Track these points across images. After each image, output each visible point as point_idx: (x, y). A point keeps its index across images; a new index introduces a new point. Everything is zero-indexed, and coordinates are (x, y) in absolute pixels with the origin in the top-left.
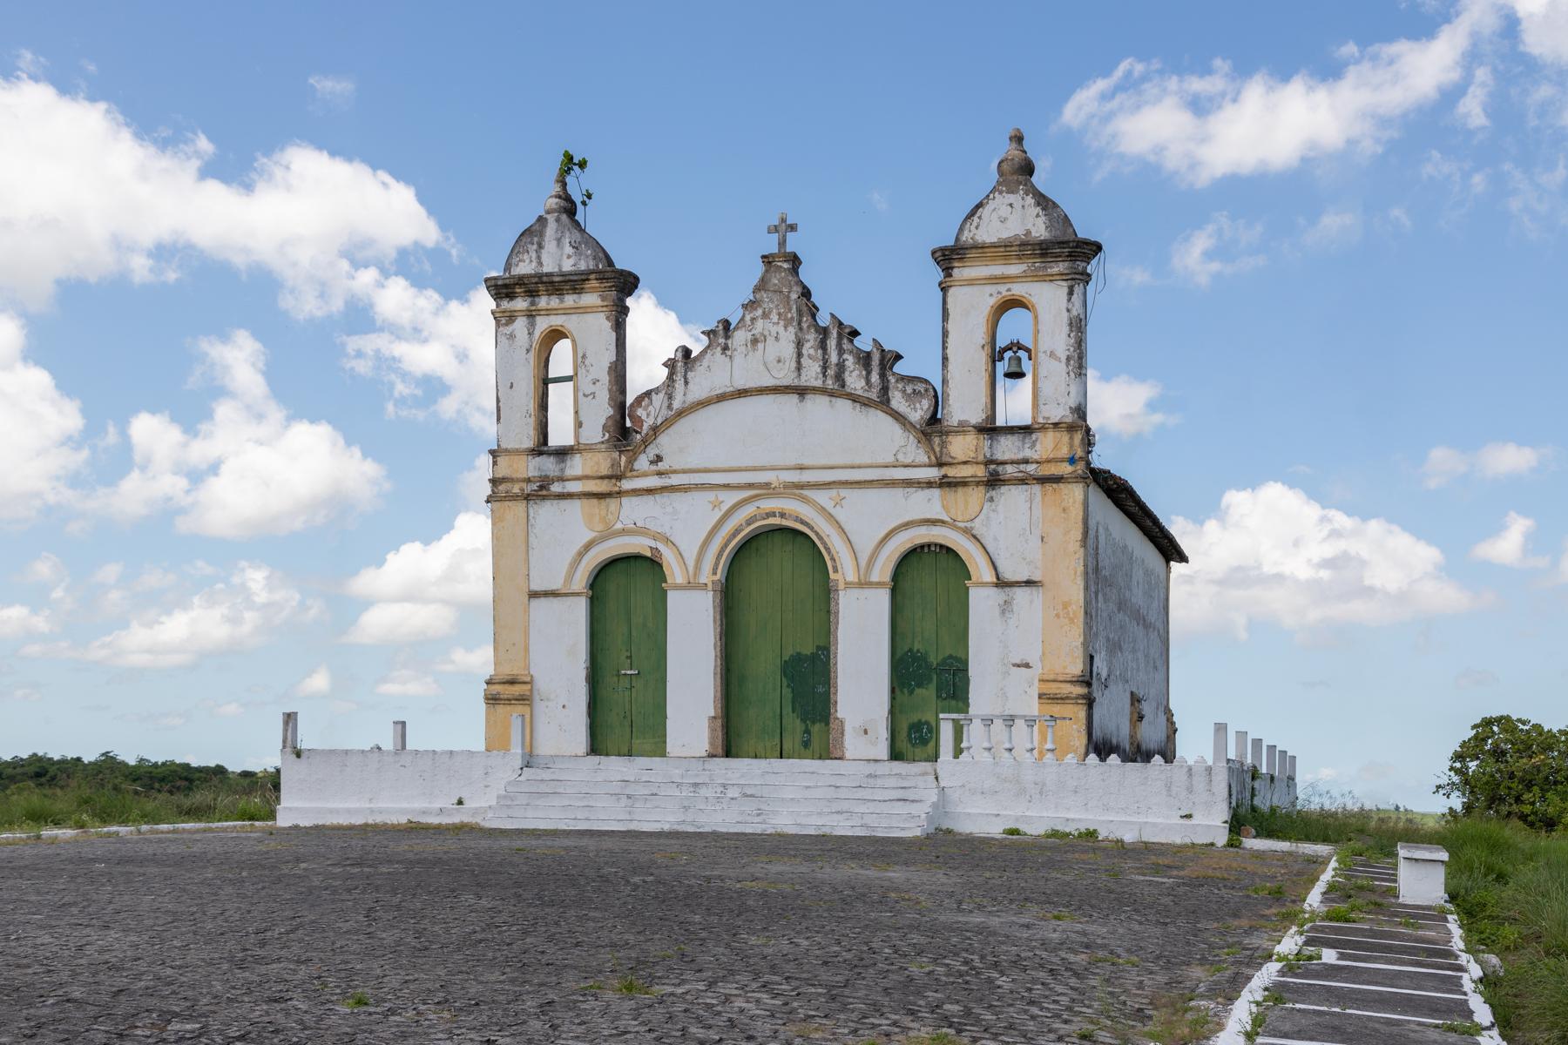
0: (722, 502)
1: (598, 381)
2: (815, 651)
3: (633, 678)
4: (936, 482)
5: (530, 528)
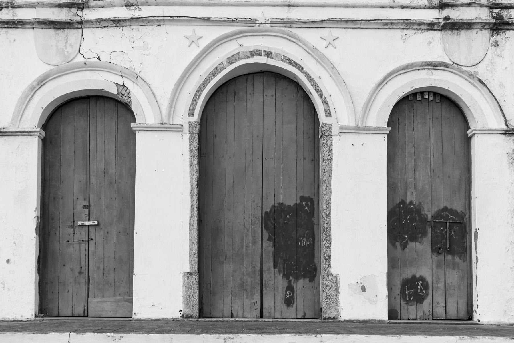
0: (201, 38)
2: (298, 202)
3: (92, 229)
4: (439, 23)
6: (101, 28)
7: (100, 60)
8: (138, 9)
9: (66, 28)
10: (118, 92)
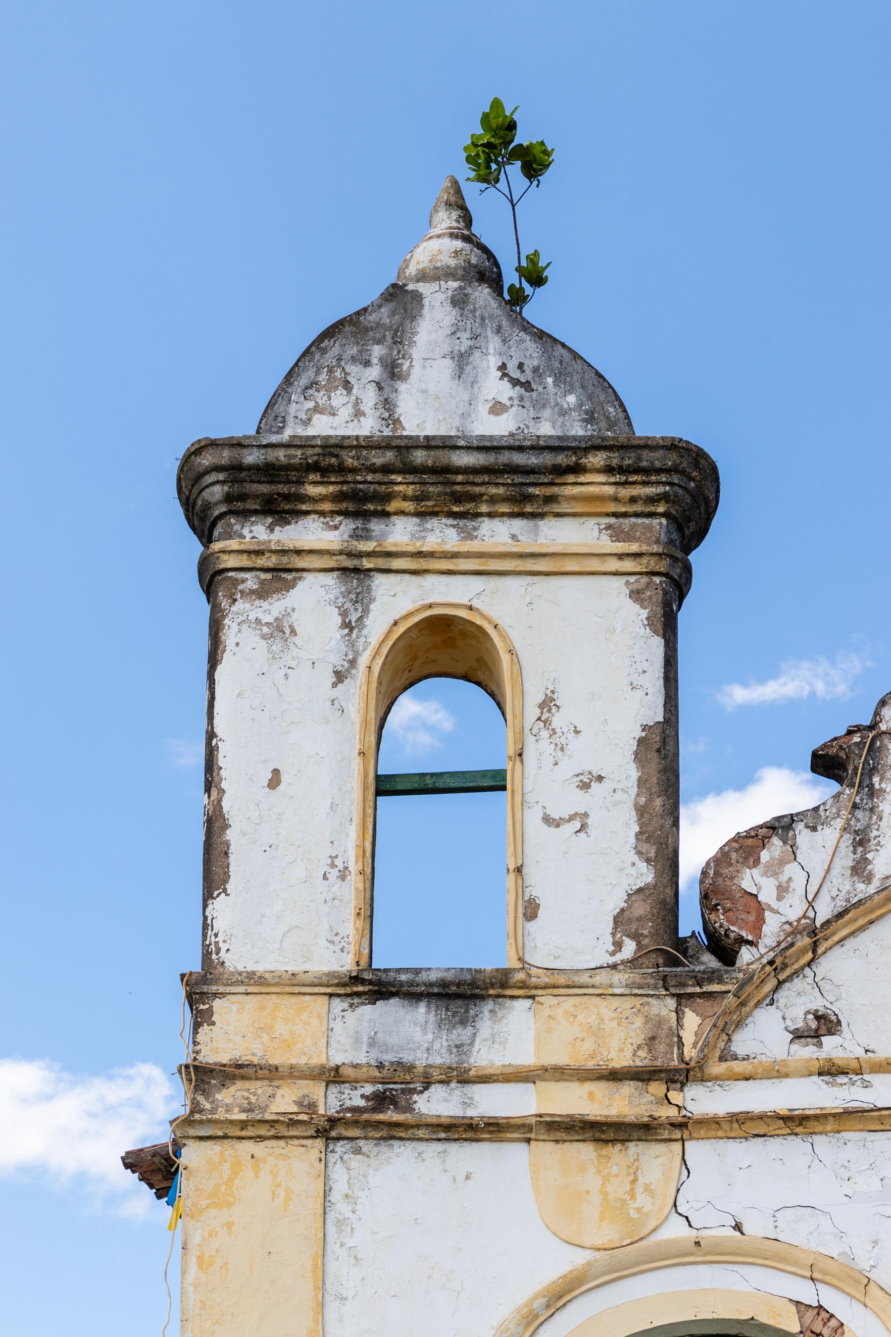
1: (600, 778)
5: (331, 1229)
6: (744, 1140)
7: (743, 1234)
8: (859, 1083)
9: (632, 1141)
10: (801, 1328)
